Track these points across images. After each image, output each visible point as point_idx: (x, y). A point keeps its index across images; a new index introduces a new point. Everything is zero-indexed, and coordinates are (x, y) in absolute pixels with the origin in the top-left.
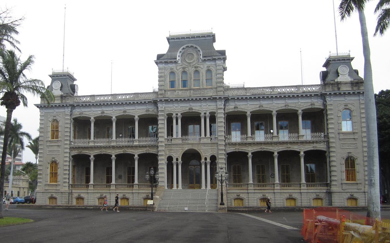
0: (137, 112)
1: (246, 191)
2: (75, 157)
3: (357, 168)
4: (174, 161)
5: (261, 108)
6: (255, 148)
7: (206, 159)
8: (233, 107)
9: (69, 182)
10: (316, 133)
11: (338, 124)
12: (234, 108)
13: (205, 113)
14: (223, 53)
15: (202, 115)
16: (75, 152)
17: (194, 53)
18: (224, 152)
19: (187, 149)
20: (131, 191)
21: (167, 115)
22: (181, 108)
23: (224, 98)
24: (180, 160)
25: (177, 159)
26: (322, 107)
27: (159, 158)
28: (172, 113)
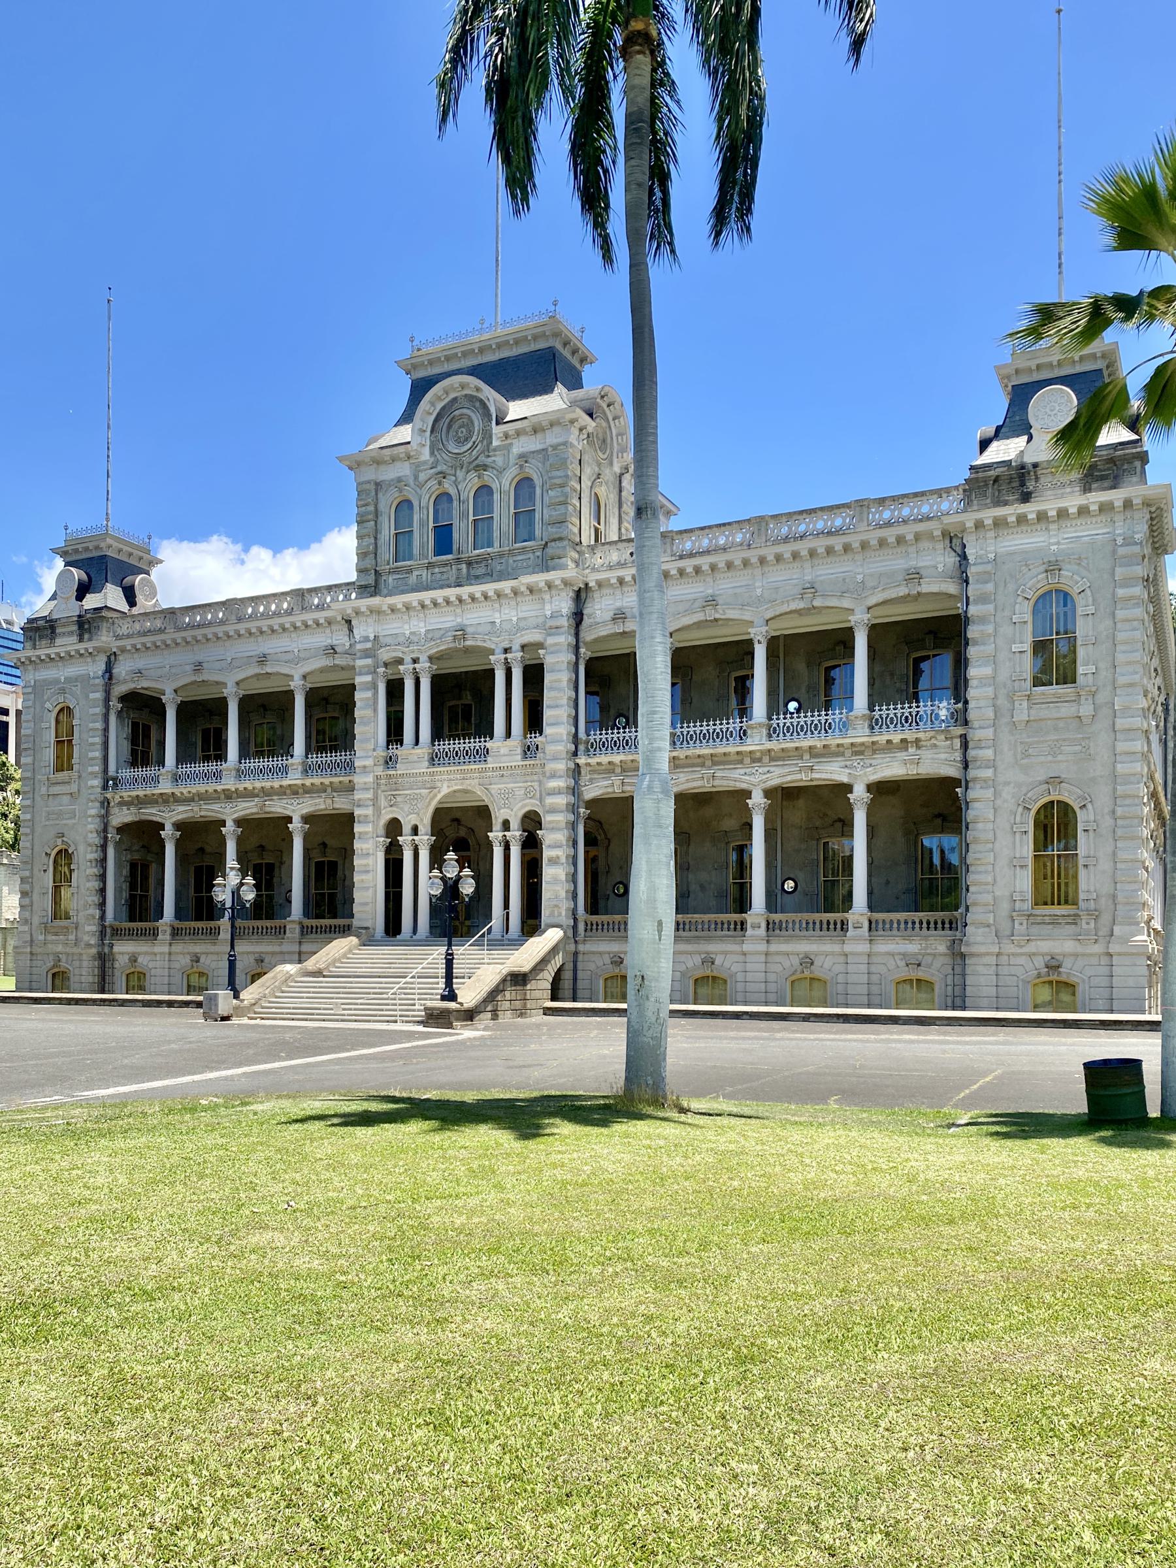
2: (122, 829)
3: (1084, 845)
5: (711, 614)
7: (506, 826)
8: (608, 615)
9: (103, 917)
10: (914, 705)
11: (1011, 655)
12: (614, 619)
16: (122, 816)
19: (445, 790)
20: (277, 949)
22: (429, 636)
25: (415, 830)
26: (952, 588)
27: (357, 828)
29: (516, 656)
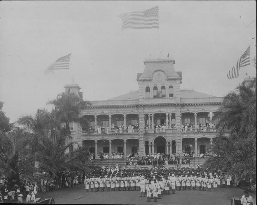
0: (124, 112)
1: (194, 162)
4: (150, 143)
5: (203, 111)
6: (199, 135)
7: (169, 143)
8: (186, 110)
13: (169, 114)
14: (180, 74)
15: (167, 114)
17: (160, 73)
18: (179, 138)
19: (157, 136)
21: (145, 115)
23: (181, 104)
24: (153, 144)
25: (151, 143)
28: (148, 113)
29: (170, 114)
